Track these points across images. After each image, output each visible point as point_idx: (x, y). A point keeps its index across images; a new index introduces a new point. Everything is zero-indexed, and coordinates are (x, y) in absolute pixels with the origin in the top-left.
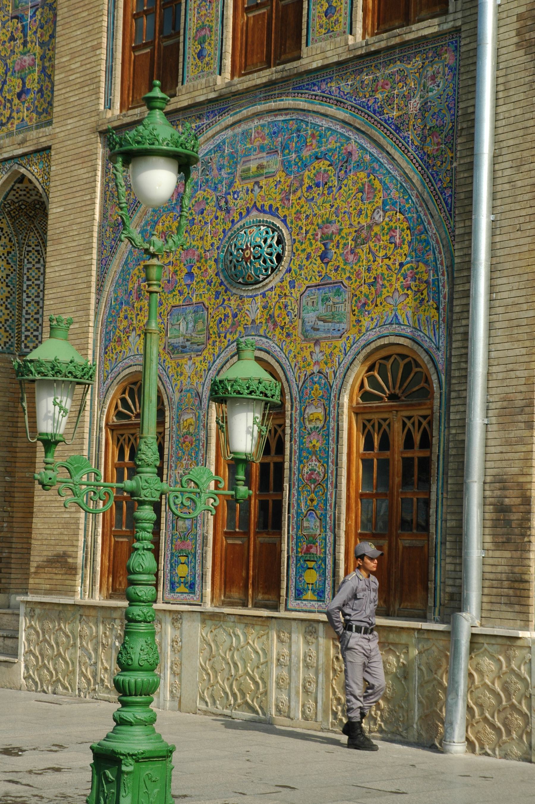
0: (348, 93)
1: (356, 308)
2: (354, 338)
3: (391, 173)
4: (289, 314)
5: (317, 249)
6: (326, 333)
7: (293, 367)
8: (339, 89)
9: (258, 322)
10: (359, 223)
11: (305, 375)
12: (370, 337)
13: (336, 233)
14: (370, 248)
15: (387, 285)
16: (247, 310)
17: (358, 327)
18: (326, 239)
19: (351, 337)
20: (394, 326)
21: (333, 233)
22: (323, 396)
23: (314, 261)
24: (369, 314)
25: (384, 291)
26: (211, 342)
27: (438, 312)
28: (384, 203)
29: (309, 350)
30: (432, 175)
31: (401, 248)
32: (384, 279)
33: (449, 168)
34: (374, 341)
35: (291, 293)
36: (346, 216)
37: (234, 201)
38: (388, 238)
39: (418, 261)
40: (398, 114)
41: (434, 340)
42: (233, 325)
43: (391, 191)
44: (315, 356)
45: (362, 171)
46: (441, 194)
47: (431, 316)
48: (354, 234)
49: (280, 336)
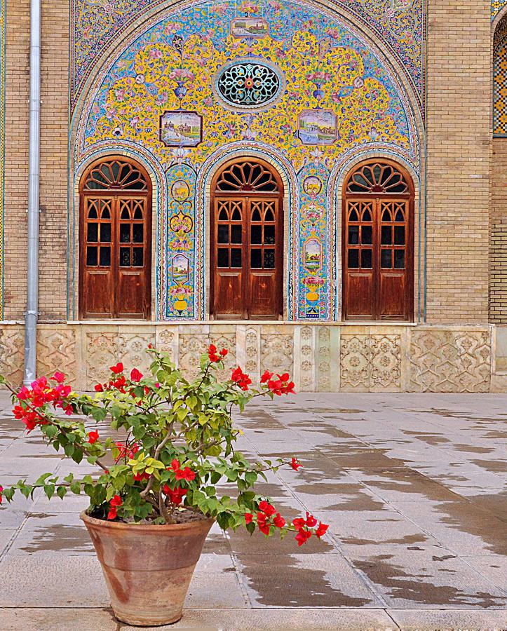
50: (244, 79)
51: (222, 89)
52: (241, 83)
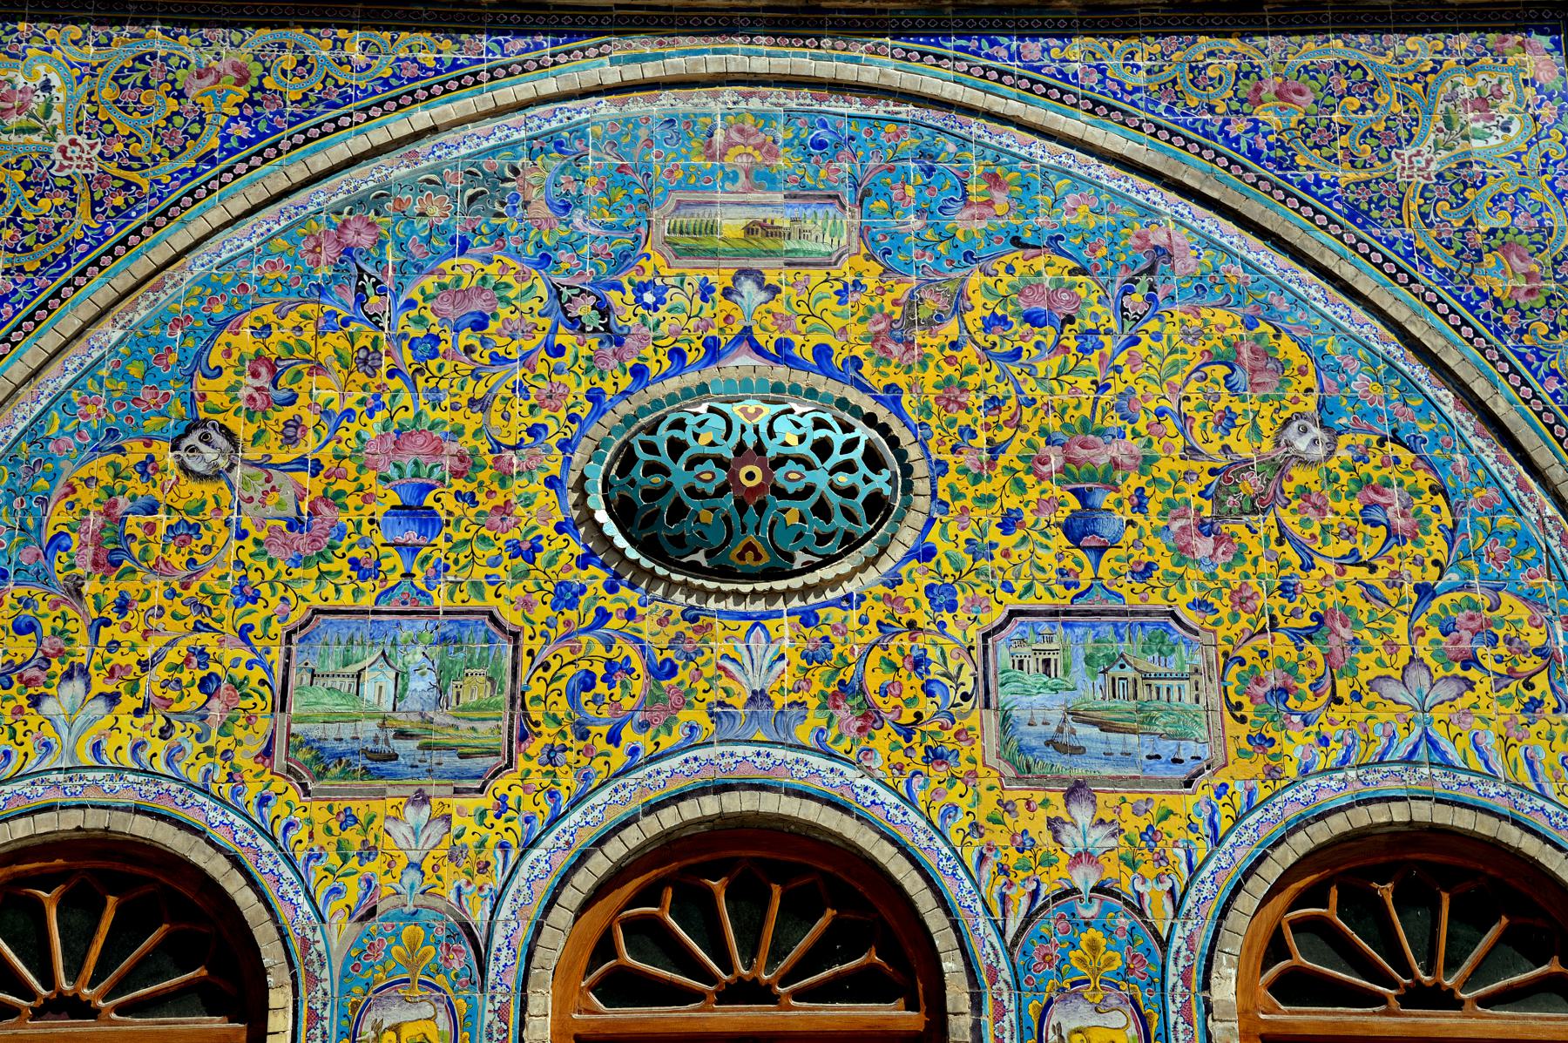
0: (1137, 90)
1: (1245, 700)
2: (1251, 794)
4: (935, 688)
5: (1043, 505)
6: (1117, 764)
7: (972, 866)
8: (1103, 72)
9: (780, 701)
11: (1034, 895)
12: (1322, 796)
13: (1129, 468)
14: (1280, 526)
15: (1376, 643)
16: (725, 656)
17: (1261, 761)
19: (1237, 787)
20: (1425, 771)
21: (1115, 464)
22: (1129, 970)
23: (1035, 535)
24: (1306, 724)
25: (1365, 660)
26: (535, 747)
29: (1041, 813)
30: (1521, 357)
31: (1417, 543)
32: (1357, 623)
34: (1340, 809)
35: (942, 625)
36: (1170, 425)
37: (640, 310)
38: (1357, 507)
39: (1497, 590)
40: (1352, 176)
42: (651, 700)
44: (1069, 836)
45: (1222, 306)
48: (1207, 479)
49: (899, 756)
50: (720, 462)
51: (623, 513)
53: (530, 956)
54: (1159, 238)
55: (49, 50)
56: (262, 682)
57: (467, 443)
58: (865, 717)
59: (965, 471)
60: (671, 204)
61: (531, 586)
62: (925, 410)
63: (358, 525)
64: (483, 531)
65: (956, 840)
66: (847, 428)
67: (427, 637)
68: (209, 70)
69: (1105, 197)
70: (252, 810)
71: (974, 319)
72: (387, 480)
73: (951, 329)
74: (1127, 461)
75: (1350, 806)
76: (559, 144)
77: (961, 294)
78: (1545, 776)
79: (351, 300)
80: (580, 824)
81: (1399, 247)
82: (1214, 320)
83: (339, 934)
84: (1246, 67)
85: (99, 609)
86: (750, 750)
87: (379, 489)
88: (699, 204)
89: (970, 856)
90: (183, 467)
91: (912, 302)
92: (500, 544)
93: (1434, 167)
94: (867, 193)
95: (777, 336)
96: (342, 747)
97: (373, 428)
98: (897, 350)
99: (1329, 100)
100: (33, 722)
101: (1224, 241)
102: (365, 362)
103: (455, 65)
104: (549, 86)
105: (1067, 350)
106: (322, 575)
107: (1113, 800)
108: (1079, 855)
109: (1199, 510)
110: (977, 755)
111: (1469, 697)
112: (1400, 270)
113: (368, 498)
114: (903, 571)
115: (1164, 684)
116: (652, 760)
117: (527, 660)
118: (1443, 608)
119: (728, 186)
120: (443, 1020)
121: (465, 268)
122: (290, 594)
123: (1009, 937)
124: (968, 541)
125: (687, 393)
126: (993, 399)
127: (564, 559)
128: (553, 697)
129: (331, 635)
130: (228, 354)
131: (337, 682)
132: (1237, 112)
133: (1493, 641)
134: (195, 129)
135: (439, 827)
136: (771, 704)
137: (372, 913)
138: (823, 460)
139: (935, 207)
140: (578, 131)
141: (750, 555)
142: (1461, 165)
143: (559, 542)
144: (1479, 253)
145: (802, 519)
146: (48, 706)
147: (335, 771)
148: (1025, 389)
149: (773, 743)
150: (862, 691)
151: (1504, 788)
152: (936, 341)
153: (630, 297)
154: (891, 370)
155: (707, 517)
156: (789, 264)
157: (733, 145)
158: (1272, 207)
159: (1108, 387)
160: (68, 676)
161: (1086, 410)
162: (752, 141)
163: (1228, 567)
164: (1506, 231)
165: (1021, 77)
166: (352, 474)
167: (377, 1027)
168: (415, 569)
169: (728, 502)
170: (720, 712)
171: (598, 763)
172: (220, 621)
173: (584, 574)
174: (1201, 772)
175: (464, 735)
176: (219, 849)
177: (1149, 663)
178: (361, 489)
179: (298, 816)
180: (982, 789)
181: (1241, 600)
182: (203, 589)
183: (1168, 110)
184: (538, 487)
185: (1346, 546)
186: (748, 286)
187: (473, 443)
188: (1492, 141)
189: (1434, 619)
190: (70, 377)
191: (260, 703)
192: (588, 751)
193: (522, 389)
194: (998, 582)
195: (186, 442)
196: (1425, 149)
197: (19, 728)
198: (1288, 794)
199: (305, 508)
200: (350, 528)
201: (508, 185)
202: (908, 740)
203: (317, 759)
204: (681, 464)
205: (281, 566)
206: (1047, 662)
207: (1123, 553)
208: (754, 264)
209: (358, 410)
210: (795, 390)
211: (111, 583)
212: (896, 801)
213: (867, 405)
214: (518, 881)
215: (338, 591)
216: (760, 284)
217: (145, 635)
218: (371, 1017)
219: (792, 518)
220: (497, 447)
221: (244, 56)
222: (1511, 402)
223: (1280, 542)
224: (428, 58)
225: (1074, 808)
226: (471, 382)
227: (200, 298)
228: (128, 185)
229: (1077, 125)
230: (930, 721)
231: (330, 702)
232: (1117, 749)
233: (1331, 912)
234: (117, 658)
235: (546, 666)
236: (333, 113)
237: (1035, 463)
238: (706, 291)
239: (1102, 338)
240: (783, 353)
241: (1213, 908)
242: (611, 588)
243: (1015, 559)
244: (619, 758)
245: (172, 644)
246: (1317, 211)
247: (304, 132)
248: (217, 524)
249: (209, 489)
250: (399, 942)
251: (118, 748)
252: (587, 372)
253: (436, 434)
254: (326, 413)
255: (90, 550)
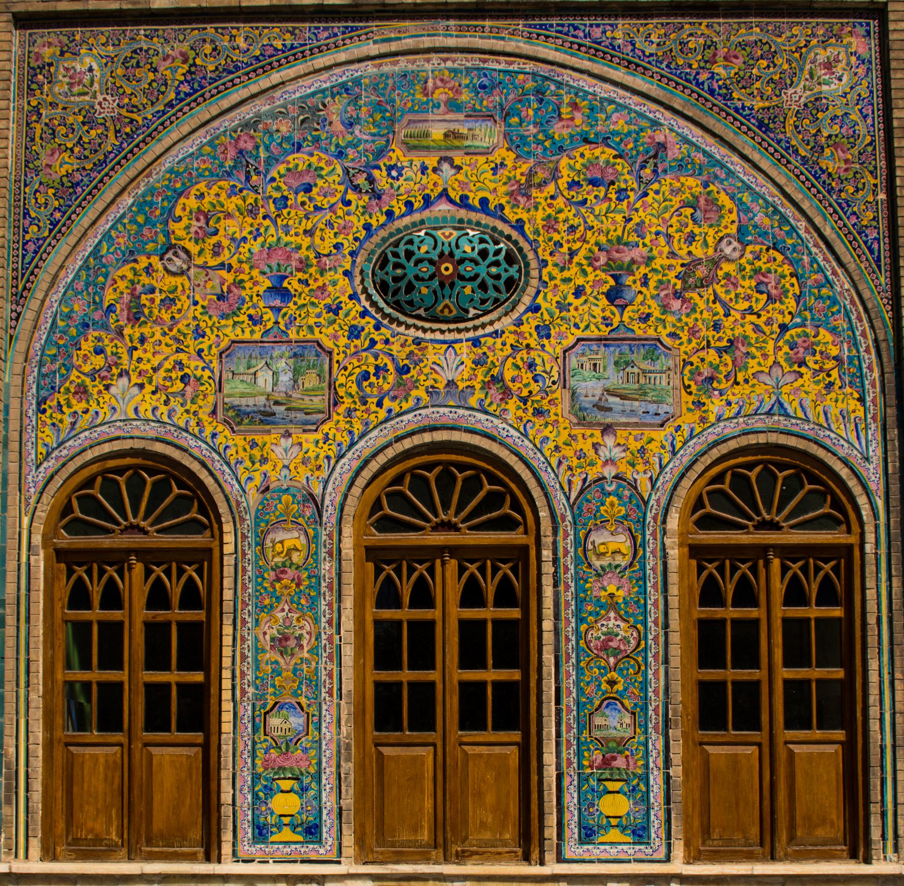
0: (651, 55)
1: (692, 383)
2: (692, 430)
3: (751, 189)
4: (539, 378)
5: (598, 283)
6: (628, 416)
7: (555, 466)
8: (633, 45)
9: (462, 385)
10: (690, 253)
12: (726, 431)
15: (758, 354)
16: (434, 363)
17: (698, 414)
18: (618, 271)
20: (776, 418)
21: (633, 261)
23: (591, 299)
24: (721, 395)
25: (752, 362)
26: (341, 409)
27: (864, 406)
28: (742, 231)
29: (590, 441)
30: (839, 205)
31: (782, 303)
32: (750, 344)
33: (870, 199)
34: (734, 437)
35: (543, 346)
36: (662, 240)
37: (390, 180)
38: (754, 284)
39: (818, 327)
40: (761, 104)
41: (857, 446)
42: (399, 385)
43: (755, 216)
44: (604, 453)
45: (691, 176)
46: (859, 233)
47: (850, 410)
48: (679, 269)
49: (520, 413)
50: (432, 262)
51: (383, 288)
52: (425, 269)
53: (342, 510)
54: (660, 138)
55: (91, 50)
56: (210, 378)
57: (303, 253)
58: (504, 393)
59: (556, 265)
60: (405, 121)
61: (337, 328)
62: (537, 232)
63: (251, 297)
64: (313, 299)
65: (547, 454)
66: (496, 243)
67: (287, 354)
68: (168, 56)
69: (633, 115)
70: (209, 440)
71: (563, 183)
72: (264, 273)
73: (551, 189)
74: (640, 260)
75: (739, 436)
76: (347, 90)
77: (557, 169)
78: (832, 419)
79: (243, 179)
80: (364, 447)
81: (783, 144)
82: (687, 184)
83: (253, 498)
84: (709, 43)
85: (131, 341)
86: (447, 410)
87: (261, 278)
88: (420, 121)
89: (554, 462)
90: (166, 269)
91: (531, 174)
92: (321, 306)
93: (803, 100)
94: (508, 114)
95: (460, 193)
96: (249, 409)
97: (256, 247)
98: (522, 200)
99: (751, 62)
100: (107, 397)
101: (694, 140)
102: (251, 211)
103: (292, 47)
104: (342, 57)
105: (610, 200)
106: (235, 323)
107: (625, 434)
108: (607, 461)
109: (675, 285)
110: (559, 412)
111: (800, 381)
112: (782, 156)
113: (256, 283)
114: (524, 318)
115: (653, 375)
116: (399, 415)
117: (336, 366)
118: (792, 336)
119: (435, 110)
120: (302, 537)
121: (299, 160)
122: (220, 333)
123: (572, 500)
124: (557, 302)
125: (414, 224)
126: (572, 226)
127: (353, 313)
128: (349, 384)
129: (240, 354)
130: (184, 209)
131: (245, 378)
132: (703, 68)
133: (814, 354)
134: (163, 89)
135: (297, 448)
136: (457, 387)
137: (267, 489)
138: (484, 260)
139: (544, 122)
140: (357, 82)
141: (446, 311)
142: (816, 100)
143: (350, 305)
144: (822, 148)
145: (473, 291)
146: (113, 390)
147: (246, 421)
148: (589, 221)
149: (458, 407)
150: (503, 380)
151: (812, 426)
152: (543, 195)
153: (384, 173)
154: (519, 211)
155: (424, 291)
156: (467, 154)
157: (437, 88)
158: (719, 121)
159: (631, 219)
160: (120, 375)
161: (619, 232)
162: (448, 85)
163: (688, 315)
164: (836, 136)
165: (590, 48)
166: (247, 271)
167: (273, 541)
168: (280, 320)
169: (435, 283)
170: (432, 391)
171: (372, 417)
172: (188, 347)
173: (363, 322)
174: (668, 420)
175: (307, 403)
176: (195, 458)
177: (646, 365)
178: (252, 278)
179: (230, 443)
180: (561, 429)
181: (693, 332)
182: (179, 331)
183: (668, 66)
184: (339, 276)
185: (746, 305)
186: (446, 166)
187: (306, 253)
188: (833, 87)
189: (787, 342)
190: (110, 224)
191: (209, 388)
192: (367, 411)
193: (330, 224)
194: (572, 324)
195: (167, 256)
196: (798, 90)
197: (101, 400)
198: (710, 430)
199: (225, 289)
200: (248, 299)
201: (321, 113)
202: (525, 404)
203: (238, 415)
204: (412, 263)
205: (215, 319)
206: (595, 365)
207: (635, 308)
208: (449, 154)
209: (249, 237)
210: (470, 222)
211: (136, 329)
212: (518, 435)
213: (507, 230)
214: (336, 474)
215: (243, 331)
216: (452, 166)
217: (154, 354)
218: (270, 537)
219: (468, 291)
220: (318, 256)
221: (185, 47)
222: (833, 228)
223: (714, 302)
224: (278, 44)
225: (606, 438)
226: (304, 221)
227: (170, 180)
228: (132, 121)
229: (619, 74)
230: (536, 395)
231: (241, 388)
232: (628, 408)
233: (726, 487)
234: (142, 366)
235: (345, 369)
236: (231, 77)
237: (592, 260)
238: (424, 169)
239: (629, 193)
240: (464, 202)
241: (670, 485)
242: (377, 328)
243: (580, 312)
244: (382, 414)
245: (166, 359)
246: (742, 124)
247: (217, 88)
248: (184, 298)
249: (179, 280)
250: (280, 502)
251: (145, 409)
252: (363, 214)
253: (288, 249)
254: (233, 239)
255: (125, 313)
